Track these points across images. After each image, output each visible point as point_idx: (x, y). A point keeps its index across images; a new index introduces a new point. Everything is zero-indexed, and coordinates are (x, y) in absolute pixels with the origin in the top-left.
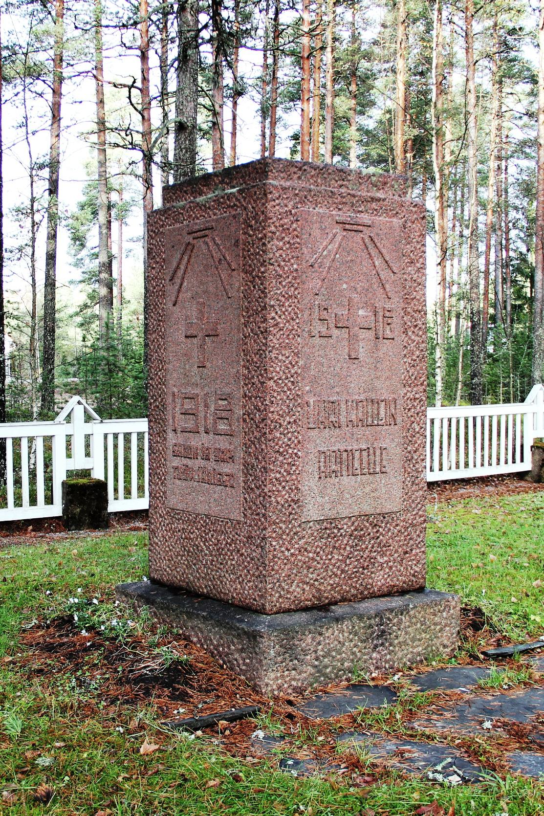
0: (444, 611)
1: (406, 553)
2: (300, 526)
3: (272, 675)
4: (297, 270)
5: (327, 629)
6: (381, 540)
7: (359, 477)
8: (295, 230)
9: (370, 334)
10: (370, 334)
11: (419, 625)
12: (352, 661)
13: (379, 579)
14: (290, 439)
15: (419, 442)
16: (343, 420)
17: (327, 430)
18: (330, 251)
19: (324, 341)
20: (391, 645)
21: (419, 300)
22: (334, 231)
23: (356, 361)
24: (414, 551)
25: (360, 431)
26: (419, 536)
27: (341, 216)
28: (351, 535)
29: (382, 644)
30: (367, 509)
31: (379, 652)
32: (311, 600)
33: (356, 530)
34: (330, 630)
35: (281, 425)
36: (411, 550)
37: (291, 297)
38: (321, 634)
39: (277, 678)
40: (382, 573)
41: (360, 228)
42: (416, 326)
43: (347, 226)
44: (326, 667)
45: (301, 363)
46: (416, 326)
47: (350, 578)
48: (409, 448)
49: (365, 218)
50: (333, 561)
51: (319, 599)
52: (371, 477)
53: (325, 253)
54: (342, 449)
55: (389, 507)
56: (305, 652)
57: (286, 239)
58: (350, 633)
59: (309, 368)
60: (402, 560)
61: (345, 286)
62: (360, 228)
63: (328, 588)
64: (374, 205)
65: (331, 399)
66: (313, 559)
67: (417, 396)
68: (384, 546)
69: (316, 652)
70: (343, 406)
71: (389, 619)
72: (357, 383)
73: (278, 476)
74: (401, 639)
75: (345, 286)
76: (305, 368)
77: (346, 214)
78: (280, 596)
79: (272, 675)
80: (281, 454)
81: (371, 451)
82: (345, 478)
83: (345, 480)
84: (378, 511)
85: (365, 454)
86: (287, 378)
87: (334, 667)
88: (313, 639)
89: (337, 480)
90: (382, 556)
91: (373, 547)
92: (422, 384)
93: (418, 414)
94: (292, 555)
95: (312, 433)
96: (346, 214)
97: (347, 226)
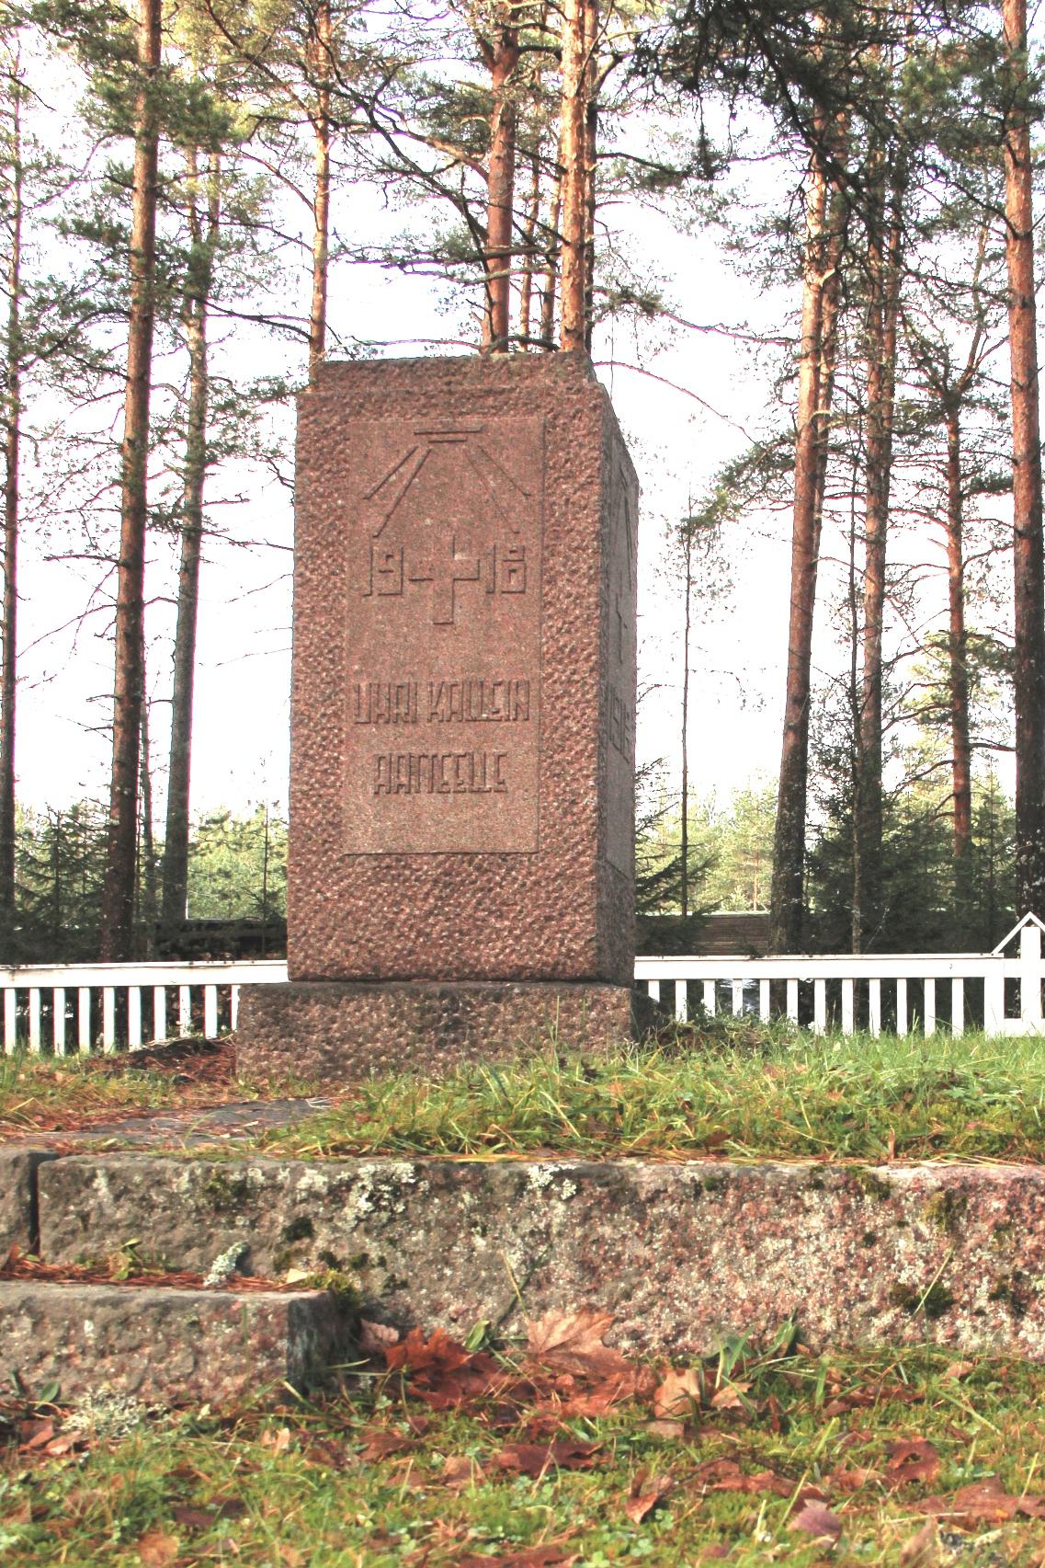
0: (590, 1009)
1: (548, 919)
2: (341, 860)
3: (252, 1052)
4: (342, 507)
5: (349, 1001)
6: (498, 894)
7: (451, 796)
8: (341, 452)
9: (479, 588)
10: (479, 588)
11: (534, 1023)
12: (395, 1056)
13: (489, 955)
14: (324, 738)
15: (578, 748)
16: (422, 710)
17: (391, 725)
18: (402, 475)
19: (385, 601)
20: (473, 1044)
21: (579, 533)
22: (411, 446)
23: (448, 628)
24: (568, 918)
25: (450, 730)
26: (579, 895)
27: (427, 423)
28: (436, 882)
29: (455, 1041)
30: (465, 843)
31: (448, 1052)
32: (358, 968)
33: (446, 874)
34: (353, 1005)
35: (310, 719)
36: (562, 915)
37: (332, 544)
38: (336, 1007)
39: (257, 1059)
40: (499, 944)
41: (461, 436)
42: (574, 572)
43: (434, 437)
44: (347, 1057)
45: (346, 633)
46: (574, 572)
47: (434, 945)
48: (557, 757)
49: (473, 421)
50: (403, 917)
51: (375, 968)
52: (475, 797)
53: (394, 478)
54: (415, 750)
55: (509, 845)
56: (309, 1029)
57: (327, 467)
58: (393, 1015)
59: (359, 640)
60: (542, 929)
61: (428, 521)
62: (461, 436)
63: (390, 951)
64: (490, 401)
65: (398, 683)
66: (365, 910)
67: (576, 677)
68: (504, 903)
69: (327, 1030)
70: (423, 694)
71: (469, 1003)
72: (450, 658)
73: (305, 788)
74: (496, 1039)
75: (428, 521)
76: (354, 640)
77: (433, 420)
78: (306, 957)
79: (252, 1052)
80: (311, 758)
81: (477, 758)
82: (423, 795)
83: (424, 798)
84: (489, 849)
85: (464, 763)
86: (321, 654)
87: (360, 1061)
88: (323, 1013)
89: (409, 798)
90: (501, 917)
91: (479, 903)
92: (587, 659)
93: (577, 704)
94: (326, 899)
95: (364, 730)
96: (433, 420)
97: (434, 437)
